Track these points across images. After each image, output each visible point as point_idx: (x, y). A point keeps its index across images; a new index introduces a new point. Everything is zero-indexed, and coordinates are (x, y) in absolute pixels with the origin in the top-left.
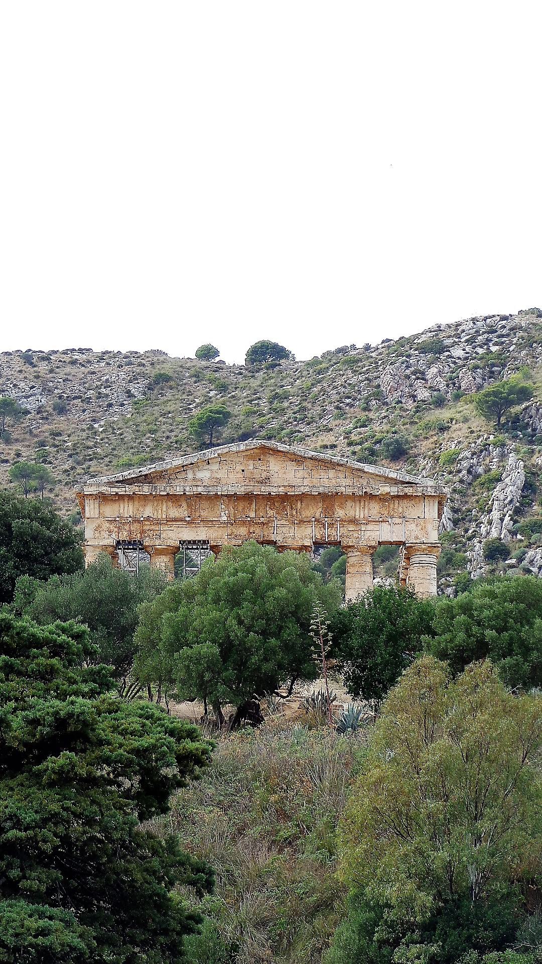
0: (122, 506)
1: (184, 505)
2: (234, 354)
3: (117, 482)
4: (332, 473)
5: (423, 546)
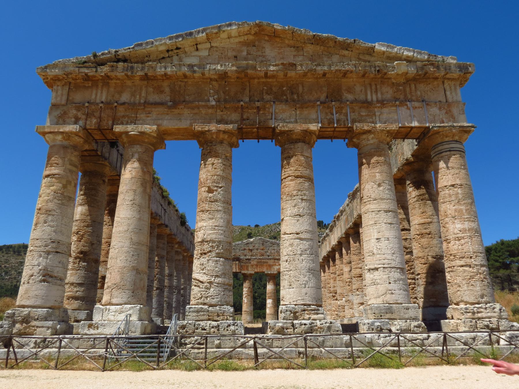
0: (94, 92)
1: (167, 90)
2: (253, 226)
3: (85, 62)
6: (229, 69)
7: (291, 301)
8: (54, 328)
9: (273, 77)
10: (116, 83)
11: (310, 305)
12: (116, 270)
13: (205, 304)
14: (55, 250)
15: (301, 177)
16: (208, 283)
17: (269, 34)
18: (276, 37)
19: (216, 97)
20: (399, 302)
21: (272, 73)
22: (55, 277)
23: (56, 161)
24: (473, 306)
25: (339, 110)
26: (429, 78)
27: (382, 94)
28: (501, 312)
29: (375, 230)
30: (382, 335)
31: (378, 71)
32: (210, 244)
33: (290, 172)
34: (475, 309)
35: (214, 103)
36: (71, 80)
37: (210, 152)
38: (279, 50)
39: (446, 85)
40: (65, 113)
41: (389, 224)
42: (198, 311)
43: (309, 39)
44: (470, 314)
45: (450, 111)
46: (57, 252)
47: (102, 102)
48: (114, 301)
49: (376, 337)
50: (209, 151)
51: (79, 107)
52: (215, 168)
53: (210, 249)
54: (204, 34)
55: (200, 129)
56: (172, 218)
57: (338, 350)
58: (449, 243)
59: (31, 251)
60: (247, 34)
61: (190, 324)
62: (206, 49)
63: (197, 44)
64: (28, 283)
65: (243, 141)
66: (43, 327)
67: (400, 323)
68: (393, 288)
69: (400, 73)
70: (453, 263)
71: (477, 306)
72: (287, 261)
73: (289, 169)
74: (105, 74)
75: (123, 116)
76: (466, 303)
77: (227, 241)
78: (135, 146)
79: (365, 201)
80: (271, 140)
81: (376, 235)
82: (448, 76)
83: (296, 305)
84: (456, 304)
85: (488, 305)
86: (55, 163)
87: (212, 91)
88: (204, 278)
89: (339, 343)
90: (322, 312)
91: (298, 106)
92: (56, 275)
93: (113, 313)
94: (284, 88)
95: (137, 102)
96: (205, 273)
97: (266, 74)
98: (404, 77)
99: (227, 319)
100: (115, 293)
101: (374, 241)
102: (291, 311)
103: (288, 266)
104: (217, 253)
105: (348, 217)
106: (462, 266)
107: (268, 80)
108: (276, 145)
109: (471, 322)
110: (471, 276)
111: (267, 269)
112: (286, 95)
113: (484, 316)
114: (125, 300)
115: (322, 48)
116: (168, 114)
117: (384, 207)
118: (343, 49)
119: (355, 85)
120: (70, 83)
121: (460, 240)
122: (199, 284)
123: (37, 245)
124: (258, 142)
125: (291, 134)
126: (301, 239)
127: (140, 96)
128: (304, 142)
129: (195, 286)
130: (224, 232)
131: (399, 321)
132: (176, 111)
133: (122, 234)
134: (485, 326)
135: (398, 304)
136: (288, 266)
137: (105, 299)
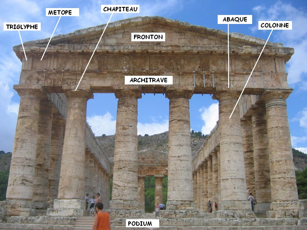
0: (49, 62)
4: (206, 41)
5: (279, 92)
6: (136, 48)
7: (174, 199)
8: (30, 212)
9: (165, 53)
10: (63, 56)
11: (185, 201)
12: (66, 178)
13: (121, 199)
14: (28, 165)
15: (182, 120)
16: (123, 187)
17: (163, 24)
18: (167, 26)
19: (127, 66)
20: (240, 199)
21: (164, 51)
22: (29, 181)
23: (26, 108)
24: (284, 202)
25: (207, 76)
26: (266, 56)
27: (235, 66)
28: (300, 206)
29: (227, 155)
30: (228, 219)
31: (233, 51)
32: (124, 163)
33: (175, 117)
34: (285, 204)
35: (126, 70)
36: (34, 54)
37: (123, 103)
38: (169, 35)
39: (276, 60)
40: (31, 76)
41: (236, 151)
42: (117, 204)
43: (188, 28)
44: (281, 207)
45: (278, 78)
46: (29, 166)
47: (54, 69)
48: (66, 197)
49: (224, 220)
50: (123, 102)
51: (39, 73)
52: (127, 114)
53: (124, 166)
54: (120, 25)
55: (117, 88)
56: (88, 137)
57: (201, 227)
58: (272, 163)
59: (13, 165)
60: (148, 24)
61: (113, 211)
62: (121, 33)
63: (115, 31)
64: (13, 184)
65: (145, 94)
66: (24, 211)
67: (240, 212)
68: (237, 191)
69: (247, 53)
70: (275, 176)
71: (287, 202)
72: (172, 174)
73: (174, 115)
74: (57, 51)
75: (68, 79)
76: (280, 201)
77: (134, 161)
78: (76, 98)
79: (222, 136)
80: (162, 94)
81: (228, 158)
82: (277, 55)
83: (177, 201)
84: (275, 201)
85: (294, 202)
86: (26, 109)
87: (125, 62)
88: (120, 184)
89: (202, 223)
90: (193, 205)
91: (180, 73)
92: (29, 180)
93: (65, 204)
94: (172, 61)
95: (77, 69)
96: (121, 181)
97: (160, 52)
98: (249, 55)
99: (135, 209)
100: (66, 192)
101: (226, 162)
102: (174, 205)
103: (172, 177)
104: (128, 169)
105: (216, 138)
106: (280, 178)
107: (162, 55)
108: (166, 97)
109: (282, 212)
110: (284, 184)
111: (156, 173)
112: (173, 66)
113: (290, 208)
114: (72, 196)
115: (197, 34)
116: (96, 77)
117: (233, 141)
118: (211, 35)
119: (218, 60)
120: (33, 56)
121: (279, 162)
122: (118, 187)
123: (17, 161)
124: (154, 95)
125: (176, 92)
126: (181, 161)
127: (78, 65)
128: (184, 97)
129: (115, 188)
130: (133, 155)
131: (239, 211)
132: (102, 76)
133: (69, 156)
134: (290, 214)
135: (239, 201)
136: (172, 177)
137: (60, 195)
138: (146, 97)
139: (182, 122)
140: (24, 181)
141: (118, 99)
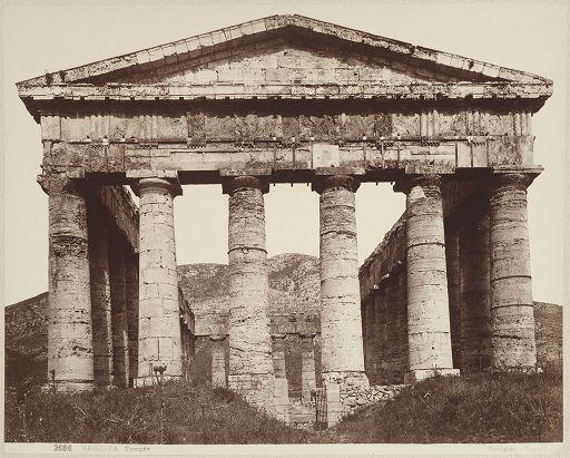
15: (345, 233)
46: (82, 322)
95: (149, 137)
138: (279, 190)
139: (345, 236)
140: (77, 349)
141: (228, 196)
